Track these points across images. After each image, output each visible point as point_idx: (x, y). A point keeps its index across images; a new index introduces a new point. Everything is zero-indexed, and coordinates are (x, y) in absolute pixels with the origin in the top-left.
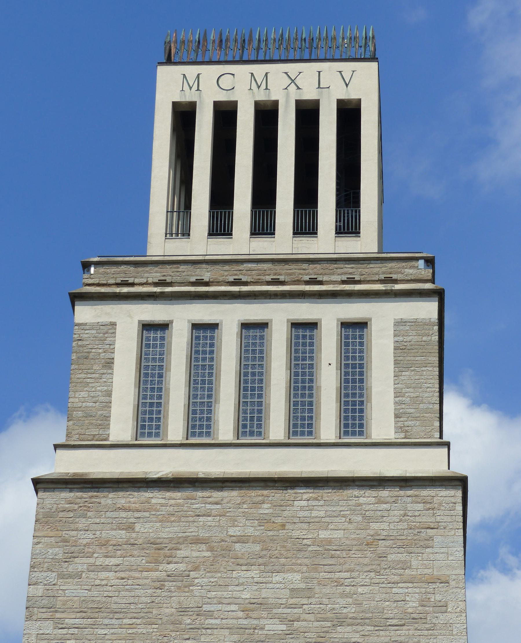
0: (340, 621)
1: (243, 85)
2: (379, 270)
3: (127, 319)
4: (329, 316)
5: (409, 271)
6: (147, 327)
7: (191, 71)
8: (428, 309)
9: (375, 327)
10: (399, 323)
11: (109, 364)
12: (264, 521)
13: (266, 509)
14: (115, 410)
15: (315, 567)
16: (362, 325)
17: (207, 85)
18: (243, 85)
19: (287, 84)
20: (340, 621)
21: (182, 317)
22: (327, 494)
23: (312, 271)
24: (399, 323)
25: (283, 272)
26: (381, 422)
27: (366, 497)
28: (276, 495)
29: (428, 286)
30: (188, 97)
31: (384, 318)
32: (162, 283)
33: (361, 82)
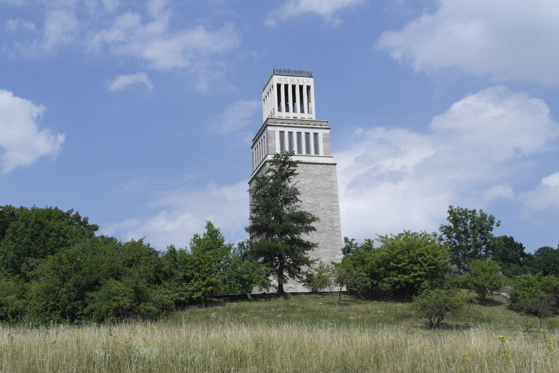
0: (318, 188)
1: (289, 80)
2: (319, 123)
3: (277, 130)
4: (312, 132)
5: (324, 124)
6: (281, 132)
7: (280, 77)
8: (328, 131)
9: (319, 134)
10: (323, 134)
11: (275, 139)
12: (304, 170)
13: (305, 168)
14: (277, 148)
15: (314, 179)
16: (317, 134)
17: (284, 80)
18: (289, 80)
19: (298, 81)
20: (318, 188)
21: (287, 130)
22: (315, 165)
23: (308, 123)
24: (323, 134)
25: (303, 122)
26: (321, 153)
27: (321, 166)
28: (306, 165)
29: (328, 127)
30: (279, 83)
31: (321, 132)
32: (282, 123)
33: (310, 82)
